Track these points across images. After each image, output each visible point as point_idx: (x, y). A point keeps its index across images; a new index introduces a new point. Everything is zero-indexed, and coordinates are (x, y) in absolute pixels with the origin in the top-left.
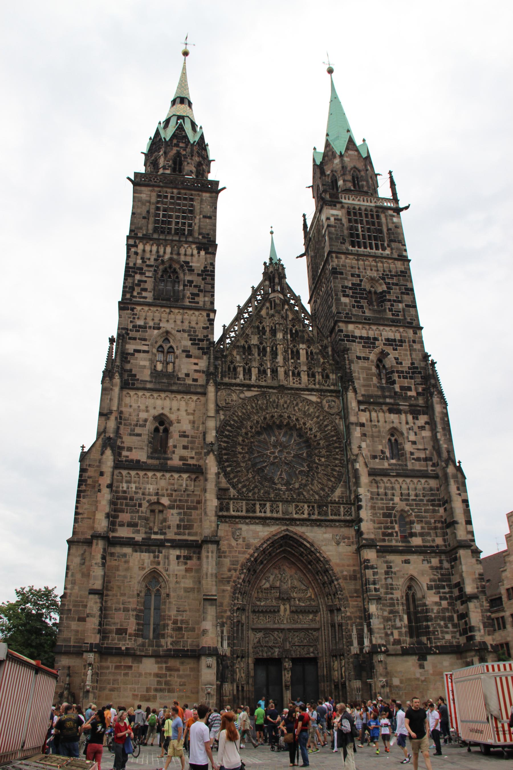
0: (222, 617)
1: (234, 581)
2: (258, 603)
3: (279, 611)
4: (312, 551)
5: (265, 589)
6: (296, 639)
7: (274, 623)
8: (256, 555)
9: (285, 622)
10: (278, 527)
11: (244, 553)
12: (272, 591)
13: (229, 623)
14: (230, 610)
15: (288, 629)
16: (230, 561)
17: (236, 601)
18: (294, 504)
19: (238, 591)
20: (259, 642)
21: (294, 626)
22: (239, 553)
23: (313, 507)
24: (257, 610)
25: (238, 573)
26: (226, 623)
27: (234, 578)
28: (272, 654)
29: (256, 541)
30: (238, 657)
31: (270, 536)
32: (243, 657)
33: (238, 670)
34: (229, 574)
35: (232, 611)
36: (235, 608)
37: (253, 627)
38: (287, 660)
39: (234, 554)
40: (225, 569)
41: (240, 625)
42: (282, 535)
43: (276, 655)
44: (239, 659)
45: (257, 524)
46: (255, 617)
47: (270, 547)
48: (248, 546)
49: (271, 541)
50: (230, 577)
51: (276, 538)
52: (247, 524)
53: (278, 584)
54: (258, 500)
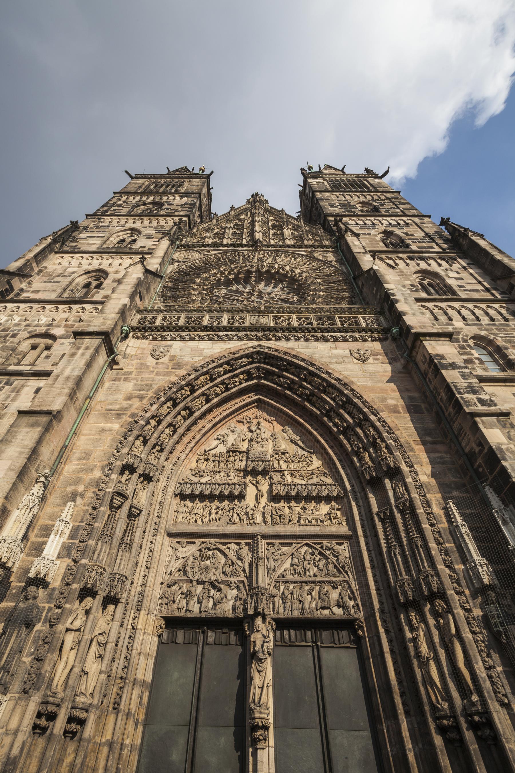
0: (77, 481)
1: (133, 415)
2: (195, 479)
3: (241, 497)
4: (312, 374)
5: (215, 455)
6: (287, 564)
7: (231, 522)
8: (192, 376)
9: (259, 519)
10: (241, 343)
11: (167, 374)
12: (231, 459)
13: (89, 494)
14: (103, 468)
15: (265, 537)
16: (135, 385)
17: (125, 450)
18: (271, 315)
19: (135, 432)
20: (183, 570)
21: (280, 529)
22: (157, 374)
23: (308, 318)
24: (188, 492)
25: (145, 402)
26: (82, 496)
27: (133, 410)
28: (215, 604)
29: (196, 359)
30: (87, 592)
31: (225, 353)
32: (111, 600)
33: (70, 639)
34: (125, 404)
35: (108, 469)
36: (119, 463)
37: (174, 530)
38: (259, 621)
39: (146, 375)
40: (121, 396)
41: (125, 509)
42: (248, 352)
43: (226, 609)
44: (88, 601)
45: (201, 338)
46: (182, 509)
47: (226, 372)
48: (178, 366)
49: (227, 359)
50: (126, 409)
51: (236, 356)
52: (183, 339)
53: (244, 446)
54: (207, 312)
